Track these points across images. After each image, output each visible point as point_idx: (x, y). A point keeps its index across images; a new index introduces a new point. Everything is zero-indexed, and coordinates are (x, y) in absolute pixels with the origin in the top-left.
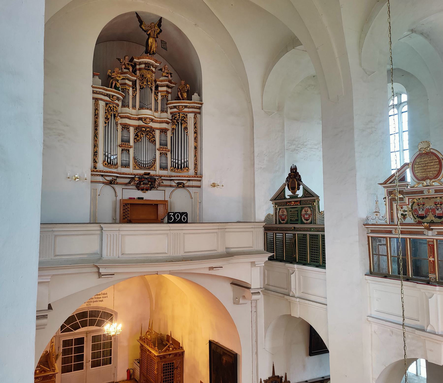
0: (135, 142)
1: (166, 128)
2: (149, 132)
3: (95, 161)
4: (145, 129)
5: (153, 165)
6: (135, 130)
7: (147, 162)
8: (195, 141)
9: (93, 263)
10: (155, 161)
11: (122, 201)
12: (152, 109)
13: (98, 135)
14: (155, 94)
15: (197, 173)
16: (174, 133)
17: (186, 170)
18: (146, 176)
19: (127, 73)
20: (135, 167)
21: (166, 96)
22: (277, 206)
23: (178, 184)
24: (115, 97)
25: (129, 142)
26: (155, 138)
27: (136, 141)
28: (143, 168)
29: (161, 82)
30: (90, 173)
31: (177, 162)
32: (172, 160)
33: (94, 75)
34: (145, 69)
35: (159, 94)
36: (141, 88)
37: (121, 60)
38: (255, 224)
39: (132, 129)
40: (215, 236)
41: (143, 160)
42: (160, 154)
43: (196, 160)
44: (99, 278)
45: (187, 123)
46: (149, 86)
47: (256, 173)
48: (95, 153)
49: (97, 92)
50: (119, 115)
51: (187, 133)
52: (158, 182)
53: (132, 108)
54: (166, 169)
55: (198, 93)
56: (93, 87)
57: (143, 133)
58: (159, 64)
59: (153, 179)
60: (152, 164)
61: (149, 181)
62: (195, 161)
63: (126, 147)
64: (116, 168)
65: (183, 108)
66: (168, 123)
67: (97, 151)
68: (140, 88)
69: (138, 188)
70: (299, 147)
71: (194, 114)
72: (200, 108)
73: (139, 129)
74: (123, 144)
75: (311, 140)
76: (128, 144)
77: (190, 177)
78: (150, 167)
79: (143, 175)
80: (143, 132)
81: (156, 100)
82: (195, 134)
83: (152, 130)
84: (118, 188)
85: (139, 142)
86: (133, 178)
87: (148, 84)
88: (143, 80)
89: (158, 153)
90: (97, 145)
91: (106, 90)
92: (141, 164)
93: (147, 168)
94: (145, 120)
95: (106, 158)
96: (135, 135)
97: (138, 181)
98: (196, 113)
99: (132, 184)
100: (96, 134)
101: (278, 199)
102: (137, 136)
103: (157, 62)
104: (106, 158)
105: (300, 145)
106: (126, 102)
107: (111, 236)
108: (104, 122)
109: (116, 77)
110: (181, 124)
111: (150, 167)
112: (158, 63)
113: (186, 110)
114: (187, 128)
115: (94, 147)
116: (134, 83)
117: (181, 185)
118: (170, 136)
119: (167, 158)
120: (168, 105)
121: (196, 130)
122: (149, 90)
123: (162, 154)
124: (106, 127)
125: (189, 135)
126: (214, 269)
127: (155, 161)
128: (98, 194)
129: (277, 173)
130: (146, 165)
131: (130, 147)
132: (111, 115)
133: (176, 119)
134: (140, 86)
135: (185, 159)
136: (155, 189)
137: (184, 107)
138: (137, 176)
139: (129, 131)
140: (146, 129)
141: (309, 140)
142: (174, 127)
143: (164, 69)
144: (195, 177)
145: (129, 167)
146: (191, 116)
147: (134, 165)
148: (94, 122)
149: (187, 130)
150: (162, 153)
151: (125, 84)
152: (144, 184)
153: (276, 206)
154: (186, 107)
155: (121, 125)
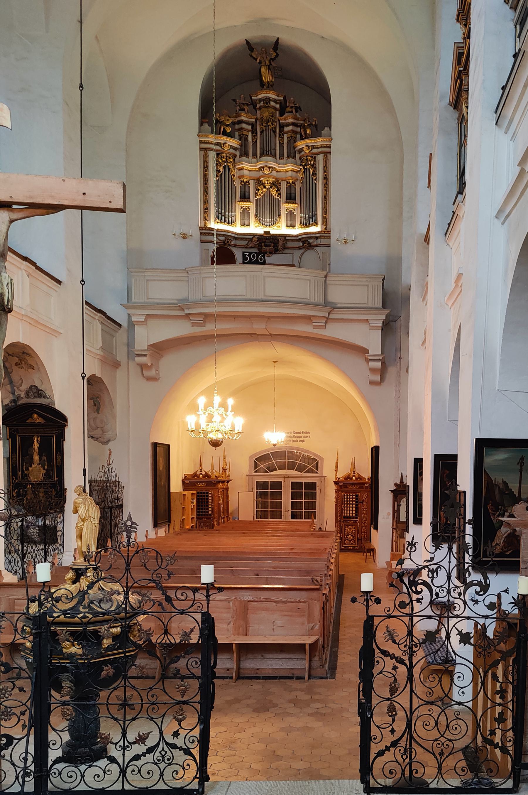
21: (292, 137)
25: (250, 199)
34: (265, 107)
35: (285, 136)
36: (262, 132)
45: (315, 167)
81: (281, 145)
97: (258, 242)
102: (257, 190)
110: (309, 169)
113: (315, 151)
114: (316, 174)
121: (325, 175)
146: (320, 157)
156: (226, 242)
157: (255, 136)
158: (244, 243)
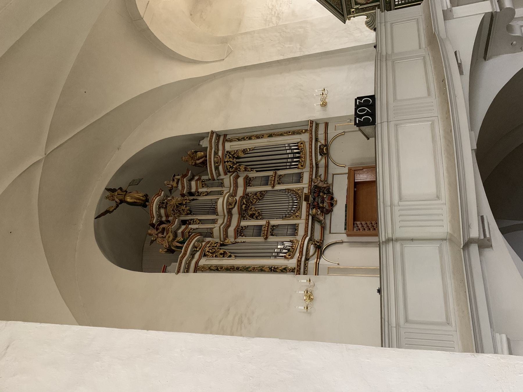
0: (261, 218)
1: (244, 178)
2: (249, 200)
3: (284, 270)
4: (243, 204)
5: (294, 192)
6: (245, 218)
7: (290, 201)
8: (262, 138)
9: (460, 251)
10: (290, 190)
11: (349, 233)
12: (218, 197)
13: (246, 266)
14: (199, 196)
15: (306, 129)
16: (251, 168)
17: (302, 145)
18: (311, 199)
19: (168, 230)
20: (296, 216)
21: (202, 181)
22: (353, 10)
23: (321, 153)
24: (196, 244)
25: (261, 226)
26: (257, 192)
27: (260, 217)
28: (299, 205)
29: (184, 188)
30: (302, 276)
31: (291, 159)
32: (288, 167)
33: (164, 271)
34: (166, 208)
35: (200, 190)
36: (190, 213)
37: (153, 240)
38: (379, 22)
39: (244, 223)
40: (398, 62)
41: (287, 204)
42: (280, 184)
43: (288, 133)
44: (491, 246)
46: (188, 203)
47: (307, 53)
48: (271, 271)
49: (187, 268)
50: (222, 240)
51: (251, 150)
52: (320, 183)
53: (215, 224)
54: (301, 174)
55: (200, 141)
56: (178, 272)
57: (249, 208)
58: (163, 192)
59: (314, 190)
60: (293, 194)
61: (319, 195)
62: (289, 134)
63: (268, 229)
64: (297, 242)
65: (217, 157)
66: (238, 177)
67: (269, 267)
68: (190, 214)
69: (329, 211)
70: (275, 13)
71: (226, 142)
72: (219, 135)
73: (244, 214)
74: (263, 233)
75: (266, 2)
76: (264, 227)
77: (312, 138)
78: (297, 196)
79: (310, 204)
80: (248, 209)
81: (208, 194)
82: (252, 139)
83: (246, 195)
84: (330, 239)
85: (263, 212)
86: (313, 218)
87: (185, 203)
88: (180, 210)
89: (278, 187)
90: (260, 267)
91: (185, 254)
92: (294, 209)
93: (299, 201)
94: (230, 204)
95: (281, 255)
96: (251, 218)
98: (225, 140)
99: (322, 218)
100: (245, 269)
101: (341, 10)
102: (253, 216)
103: (160, 194)
104: (281, 255)
105: (272, 12)
106: (207, 232)
107: (403, 221)
108: (229, 258)
109: (168, 242)
110: (238, 158)
111: (298, 197)
112: (160, 192)
113: (220, 153)
114: (244, 150)
115: (263, 272)
116: (184, 222)
117: (323, 149)
118: (255, 173)
119: (285, 174)
120: (214, 178)
122: (193, 202)
123: (280, 182)
124: (235, 256)
125: (253, 147)
126: (459, 62)
127: (288, 189)
128: (336, 266)
129: (307, 29)
130: (295, 201)
131: (267, 224)
132: (220, 249)
133: (232, 166)
134: (188, 214)
135: (288, 151)
136: (331, 187)
137: (216, 156)
138: (311, 213)
139: (245, 227)
140: (244, 204)
141: (266, 4)
142: (242, 168)
143: (168, 186)
144: (312, 130)
145: (297, 225)
146: (228, 146)
147: (294, 219)
148: (228, 272)
149: (247, 150)
150: (278, 181)
151: (183, 233)
152: (323, 202)
153: (353, 11)
154: (216, 153)
155: (237, 237)
156: (318, 244)
157: (193, 221)
158: (317, 227)
